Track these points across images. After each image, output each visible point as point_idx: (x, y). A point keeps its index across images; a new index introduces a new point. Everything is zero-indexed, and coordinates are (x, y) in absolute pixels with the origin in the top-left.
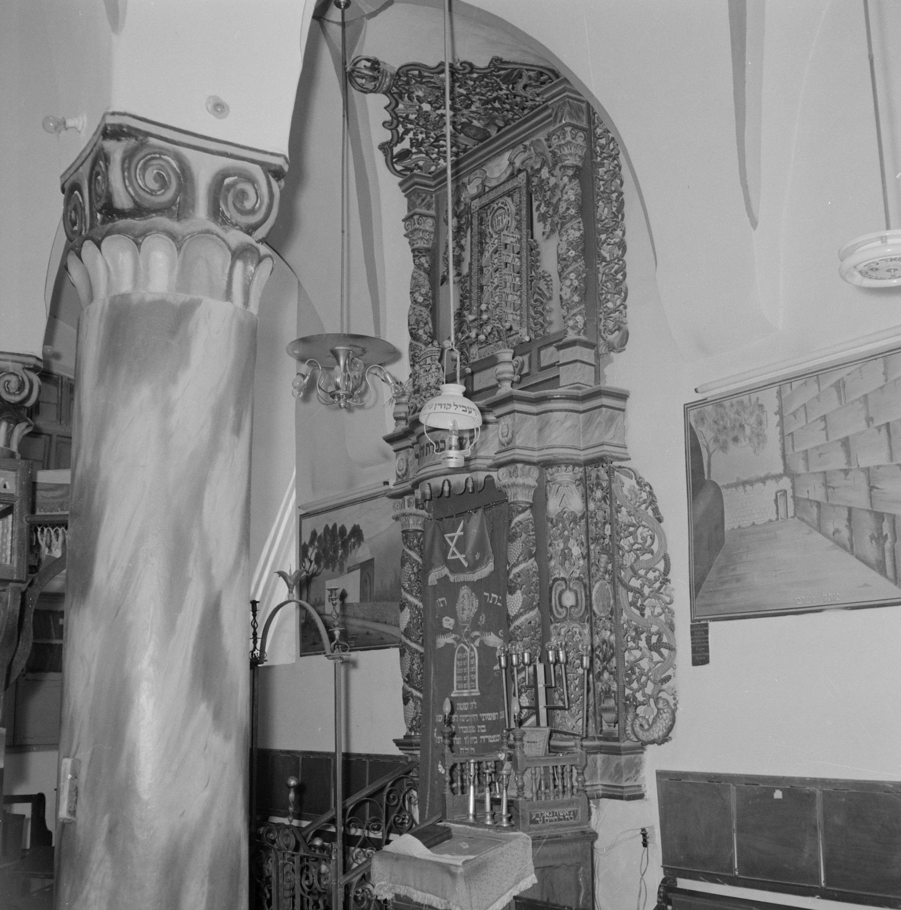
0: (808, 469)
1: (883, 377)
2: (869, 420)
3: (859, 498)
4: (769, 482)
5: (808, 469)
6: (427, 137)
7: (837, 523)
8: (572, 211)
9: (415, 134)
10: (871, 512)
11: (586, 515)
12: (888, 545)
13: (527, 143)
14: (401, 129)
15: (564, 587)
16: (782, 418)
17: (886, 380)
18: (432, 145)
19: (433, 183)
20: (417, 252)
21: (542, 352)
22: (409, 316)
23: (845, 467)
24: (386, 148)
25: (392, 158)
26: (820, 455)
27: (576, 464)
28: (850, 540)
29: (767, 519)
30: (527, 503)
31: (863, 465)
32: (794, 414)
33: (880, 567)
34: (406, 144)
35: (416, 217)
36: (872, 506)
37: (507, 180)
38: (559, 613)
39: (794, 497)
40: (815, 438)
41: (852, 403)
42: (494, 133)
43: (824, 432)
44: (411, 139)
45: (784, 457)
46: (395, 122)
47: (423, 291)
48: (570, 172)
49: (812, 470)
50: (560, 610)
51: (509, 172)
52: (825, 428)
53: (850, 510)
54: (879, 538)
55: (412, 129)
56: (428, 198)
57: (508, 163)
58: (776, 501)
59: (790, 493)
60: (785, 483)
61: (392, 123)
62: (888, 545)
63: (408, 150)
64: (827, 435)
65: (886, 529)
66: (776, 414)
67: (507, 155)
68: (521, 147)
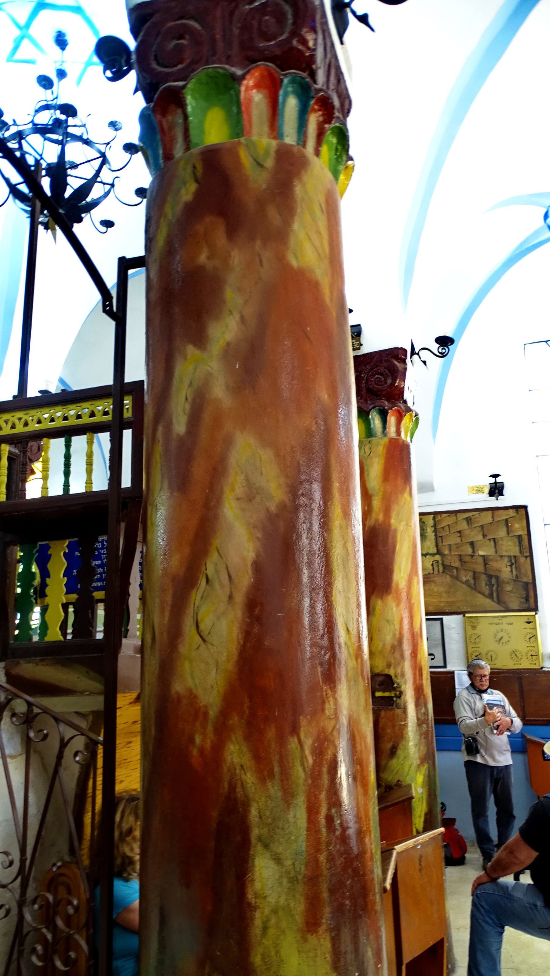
0: (450, 552)
1: (492, 519)
2: (484, 536)
3: (480, 568)
4: (428, 556)
5: (450, 552)
7: (467, 577)
10: (486, 574)
12: (494, 588)
16: (435, 528)
17: (493, 520)
23: (472, 554)
26: (457, 547)
28: (475, 584)
29: (428, 572)
31: (481, 553)
32: (443, 528)
33: (491, 596)
36: (486, 571)
39: (443, 564)
40: (454, 540)
41: (475, 527)
43: (460, 538)
45: (437, 546)
49: (452, 553)
52: (460, 536)
53: (474, 572)
54: (491, 586)
58: (432, 565)
59: (440, 562)
60: (438, 557)
62: (494, 588)
64: (461, 539)
65: (494, 581)
66: (432, 527)
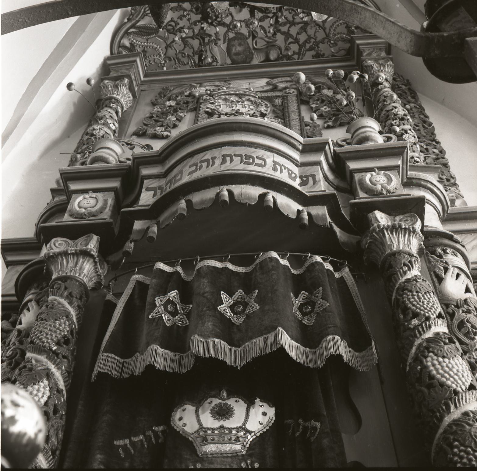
9: (181, 18)
25: (133, 26)
42: (256, 61)
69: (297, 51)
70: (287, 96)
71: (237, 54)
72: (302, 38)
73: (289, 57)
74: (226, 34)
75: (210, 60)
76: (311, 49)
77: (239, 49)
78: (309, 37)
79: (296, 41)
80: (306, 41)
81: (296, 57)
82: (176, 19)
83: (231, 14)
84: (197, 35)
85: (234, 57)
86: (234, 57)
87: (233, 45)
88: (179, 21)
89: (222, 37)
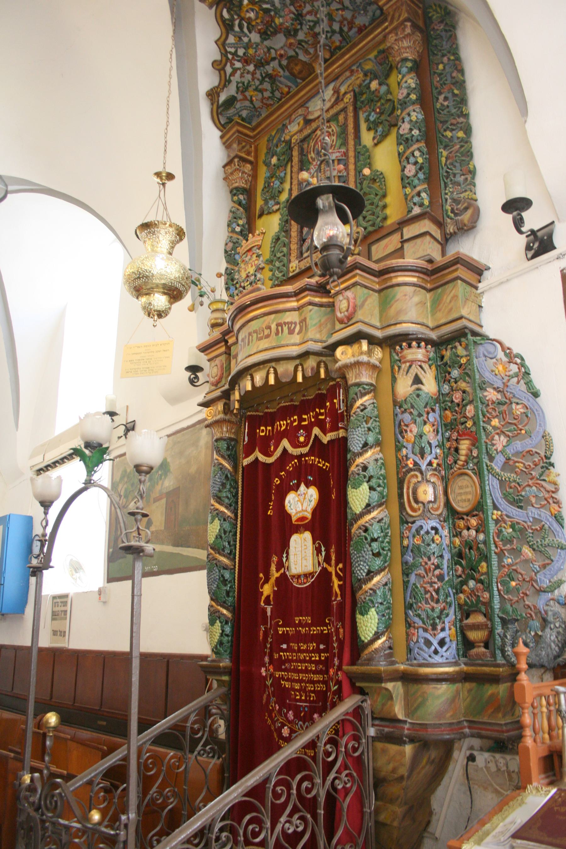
6: (253, 80)
8: (413, 97)
9: (242, 76)
11: (441, 400)
13: (354, 68)
14: (229, 70)
15: (420, 479)
18: (256, 89)
19: (251, 134)
20: (234, 192)
21: (374, 248)
22: (226, 244)
24: (212, 95)
27: (428, 341)
30: (372, 385)
34: (231, 90)
35: (236, 160)
37: (332, 107)
38: (414, 510)
44: (238, 83)
46: (224, 59)
47: (241, 222)
48: (409, 64)
50: (415, 506)
51: (333, 100)
55: (239, 69)
56: (248, 147)
57: (332, 92)
61: (221, 61)
63: (233, 96)
67: (331, 86)
68: (348, 73)
69: (340, 38)
70: (346, 107)
71: (300, 72)
72: (336, 27)
73: (339, 48)
74: (280, 65)
75: (286, 89)
76: (350, 29)
77: (298, 68)
78: (341, 22)
79: (333, 32)
80: (341, 29)
81: (344, 44)
82: (239, 80)
83: (271, 48)
84: (263, 79)
85: (300, 76)
86: (300, 76)
87: (292, 69)
88: (243, 80)
89: (280, 70)
